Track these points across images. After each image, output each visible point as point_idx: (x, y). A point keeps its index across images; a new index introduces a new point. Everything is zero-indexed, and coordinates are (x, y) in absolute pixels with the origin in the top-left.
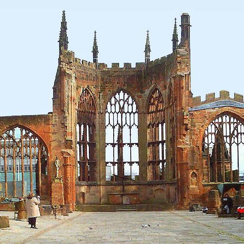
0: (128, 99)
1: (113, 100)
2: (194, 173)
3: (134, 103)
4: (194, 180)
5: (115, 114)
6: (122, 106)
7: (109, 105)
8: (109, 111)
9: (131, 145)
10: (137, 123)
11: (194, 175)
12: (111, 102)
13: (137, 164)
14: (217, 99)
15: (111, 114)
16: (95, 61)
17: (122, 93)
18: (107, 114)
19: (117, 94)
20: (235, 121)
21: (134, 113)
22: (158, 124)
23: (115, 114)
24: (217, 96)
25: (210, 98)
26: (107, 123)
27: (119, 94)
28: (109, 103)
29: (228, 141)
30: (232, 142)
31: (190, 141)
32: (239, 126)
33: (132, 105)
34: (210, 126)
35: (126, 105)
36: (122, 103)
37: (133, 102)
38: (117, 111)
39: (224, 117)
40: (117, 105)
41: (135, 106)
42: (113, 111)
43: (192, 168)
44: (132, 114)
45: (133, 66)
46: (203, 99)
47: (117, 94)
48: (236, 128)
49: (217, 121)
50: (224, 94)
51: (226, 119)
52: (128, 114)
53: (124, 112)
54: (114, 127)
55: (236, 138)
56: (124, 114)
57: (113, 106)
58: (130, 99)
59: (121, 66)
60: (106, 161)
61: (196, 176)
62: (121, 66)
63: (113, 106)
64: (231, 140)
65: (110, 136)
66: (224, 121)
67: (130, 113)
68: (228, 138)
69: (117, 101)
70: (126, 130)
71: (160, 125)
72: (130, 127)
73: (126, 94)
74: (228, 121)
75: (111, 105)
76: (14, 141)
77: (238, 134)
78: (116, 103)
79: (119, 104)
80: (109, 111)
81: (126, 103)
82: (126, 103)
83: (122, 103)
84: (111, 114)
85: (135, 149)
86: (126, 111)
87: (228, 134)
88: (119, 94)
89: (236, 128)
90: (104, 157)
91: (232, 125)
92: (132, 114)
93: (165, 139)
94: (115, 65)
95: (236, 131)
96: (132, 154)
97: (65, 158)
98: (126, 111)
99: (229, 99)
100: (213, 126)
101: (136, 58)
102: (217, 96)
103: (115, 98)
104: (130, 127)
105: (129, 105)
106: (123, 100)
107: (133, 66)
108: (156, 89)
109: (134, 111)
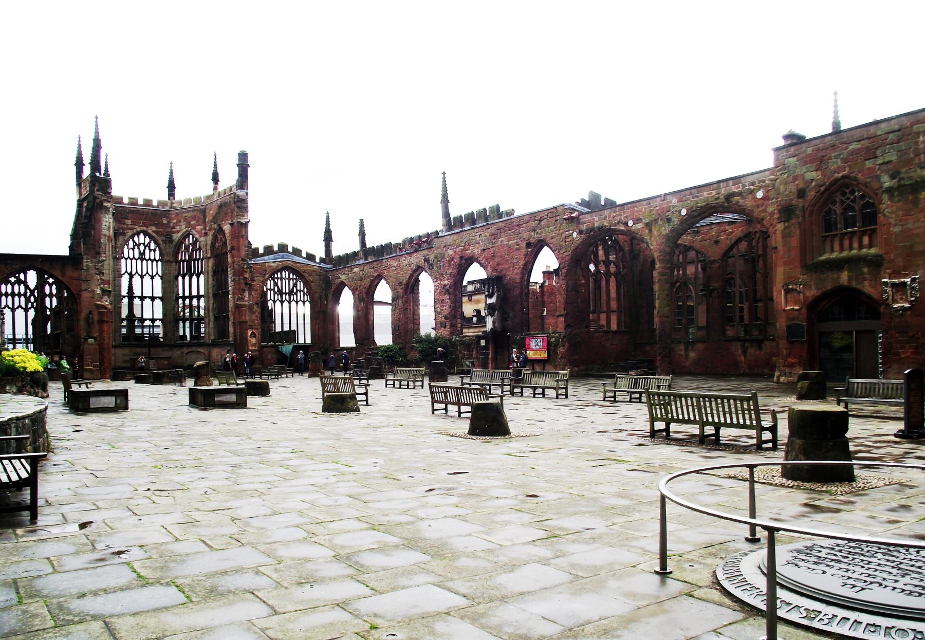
0: (149, 243)
1: (131, 244)
2: (253, 332)
3: (157, 249)
4: (254, 340)
5: (134, 261)
7: (126, 250)
8: (126, 256)
9: (153, 299)
11: (253, 335)
12: (128, 245)
14: (276, 252)
15: (129, 261)
17: (142, 236)
18: (123, 261)
19: (136, 236)
20: (295, 277)
21: (157, 261)
23: (134, 261)
24: (276, 249)
25: (269, 250)
27: (138, 237)
28: (126, 246)
29: (288, 299)
30: (292, 299)
31: (249, 298)
32: (298, 283)
33: (155, 251)
34: (269, 281)
35: (147, 251)
36: (142, 248)
38: (137, 257)
39: (283, 272)
40: (136, 250)
41: (158, 252)
42: (131, 256)
43: (251, 328)
44: (155, 263)
45: (155, 203)
46: (261, 251)
47: (136, 236)
48: (295, 285)
49: (276, 276)
50: (283, 248)
51: (285, 274)
52: (150, 262)
55: (295, 296)
56: (144, 262)
57: (131, 251)
58: (153, 246)
59: (141, 202)
61: (255, 336)
62: (141, 202)
64: (290, 298)
66: (284, 276)
67: (152, 261)
68: (287, 296)
70: (147, 279)
71: (180, 278)
72: (152, 277)
73: (147, 237)
74: (287, 277)
76: (27, 287)
77: (297, 290)
78: (134, 246)
79: (139, 248)
80: (126, 256)
81: (147, 248)
82: (147, 248)
83: (142, 248)
84: (129, 261)
85: (158, 304)
87: (287, 291)
88: (138, 237)
89: (295, 285)
91: (291, 281)
92: (155, 263)
93: (202, 292)
94: (133, 202)
95: (295, 289)
97: (100, 313)
98: (147, 258)
99: (288, 252)
100: (272, 281)
101: (159, 195)
102: (276, 249)
104: (152, 277)
105: (150, 251)
106: (144, 244)
107: (155, 203)
109: (157, 258)
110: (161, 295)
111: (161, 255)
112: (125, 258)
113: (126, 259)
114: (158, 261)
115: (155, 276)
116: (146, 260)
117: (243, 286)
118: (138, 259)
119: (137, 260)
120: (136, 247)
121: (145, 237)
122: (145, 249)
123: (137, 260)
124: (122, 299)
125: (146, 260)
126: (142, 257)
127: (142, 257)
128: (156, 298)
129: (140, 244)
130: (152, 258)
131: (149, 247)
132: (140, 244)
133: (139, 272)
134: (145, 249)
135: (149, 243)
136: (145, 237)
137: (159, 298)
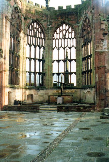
0: (68, 29)
1: (58, 31)
3: (73, 31)
5: (60, 40)
6: (64, 34)
7: (55, 34)
9: (71, 61)
10: (75, 45)
12: (57, 32)
13: (75, 74)
15: (57, 40)
16: (47, 6)
17: (64, 25)
18: (54, 41)
19: (61, 26)
21: (73, 39)
22: (88, 43)
23: (60, 40)
26: (54, 46)
27: (62, 26)
28: (55, 33)
33: (71, 33)
35: (67, 33)
36: (64, 32)
37: (72, 31)
38: (61, 38)
40: (61, 34)
41: (73, 33)
42: (58, 38)
44: (72, 40)
47: (61, 26)
52: (69, 40)
53: (66, 38)
54: (59, 49)
56: (66, 40)
58: (70, 30)
60: (54, 72)
63: (58, 35)
65: (57, 54)
67: (70, 39)
69: (61, 31)
72: (70, 48)
73: (67, 26)
75: (57, 34)
78: (60, 32)
79: (62, 33)
80: (55, 38)
81: (67, 32)
83: (64, 32)
84: (57, 40)
86: (67, 37)
88: (62, 26)
90: (51, 70)
92: (72, 40)
94: (60, 8)
96: (73, 67)
98: (67, 37)
103: (60, 29)
104: (70, 48)
105: (69, 33)
106: (65, 30)
107: (73, 7)
108: (87, 18)
109: (73, 37)
110: (75, 58)
111: (75, 35)
112: (55, 39)
113: (56, 40)
114: (74, 38)
115: (72, 47)
116: (66, 39)
117: (102, 37)
118: (62, 39)
119: (61, 39)
120: (61, 32)
121: (66, 26)
122: (66, 32)
123: (61, 39)
124: (53, 62)
125: (66, 39)
126: (64, 37)
127: (64, 37)
128: (72, 60)
129: (63, 30)
130: (70, 37)
131: (68, 32)
132: (63, 30)
133: (63, 46)
134: (66, 32)
135: (68, 29)
136: (66, 26)
137: (74, 60)
